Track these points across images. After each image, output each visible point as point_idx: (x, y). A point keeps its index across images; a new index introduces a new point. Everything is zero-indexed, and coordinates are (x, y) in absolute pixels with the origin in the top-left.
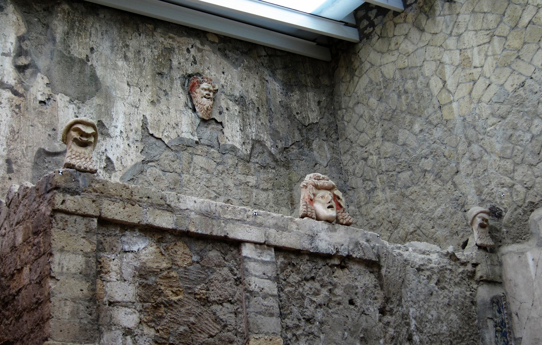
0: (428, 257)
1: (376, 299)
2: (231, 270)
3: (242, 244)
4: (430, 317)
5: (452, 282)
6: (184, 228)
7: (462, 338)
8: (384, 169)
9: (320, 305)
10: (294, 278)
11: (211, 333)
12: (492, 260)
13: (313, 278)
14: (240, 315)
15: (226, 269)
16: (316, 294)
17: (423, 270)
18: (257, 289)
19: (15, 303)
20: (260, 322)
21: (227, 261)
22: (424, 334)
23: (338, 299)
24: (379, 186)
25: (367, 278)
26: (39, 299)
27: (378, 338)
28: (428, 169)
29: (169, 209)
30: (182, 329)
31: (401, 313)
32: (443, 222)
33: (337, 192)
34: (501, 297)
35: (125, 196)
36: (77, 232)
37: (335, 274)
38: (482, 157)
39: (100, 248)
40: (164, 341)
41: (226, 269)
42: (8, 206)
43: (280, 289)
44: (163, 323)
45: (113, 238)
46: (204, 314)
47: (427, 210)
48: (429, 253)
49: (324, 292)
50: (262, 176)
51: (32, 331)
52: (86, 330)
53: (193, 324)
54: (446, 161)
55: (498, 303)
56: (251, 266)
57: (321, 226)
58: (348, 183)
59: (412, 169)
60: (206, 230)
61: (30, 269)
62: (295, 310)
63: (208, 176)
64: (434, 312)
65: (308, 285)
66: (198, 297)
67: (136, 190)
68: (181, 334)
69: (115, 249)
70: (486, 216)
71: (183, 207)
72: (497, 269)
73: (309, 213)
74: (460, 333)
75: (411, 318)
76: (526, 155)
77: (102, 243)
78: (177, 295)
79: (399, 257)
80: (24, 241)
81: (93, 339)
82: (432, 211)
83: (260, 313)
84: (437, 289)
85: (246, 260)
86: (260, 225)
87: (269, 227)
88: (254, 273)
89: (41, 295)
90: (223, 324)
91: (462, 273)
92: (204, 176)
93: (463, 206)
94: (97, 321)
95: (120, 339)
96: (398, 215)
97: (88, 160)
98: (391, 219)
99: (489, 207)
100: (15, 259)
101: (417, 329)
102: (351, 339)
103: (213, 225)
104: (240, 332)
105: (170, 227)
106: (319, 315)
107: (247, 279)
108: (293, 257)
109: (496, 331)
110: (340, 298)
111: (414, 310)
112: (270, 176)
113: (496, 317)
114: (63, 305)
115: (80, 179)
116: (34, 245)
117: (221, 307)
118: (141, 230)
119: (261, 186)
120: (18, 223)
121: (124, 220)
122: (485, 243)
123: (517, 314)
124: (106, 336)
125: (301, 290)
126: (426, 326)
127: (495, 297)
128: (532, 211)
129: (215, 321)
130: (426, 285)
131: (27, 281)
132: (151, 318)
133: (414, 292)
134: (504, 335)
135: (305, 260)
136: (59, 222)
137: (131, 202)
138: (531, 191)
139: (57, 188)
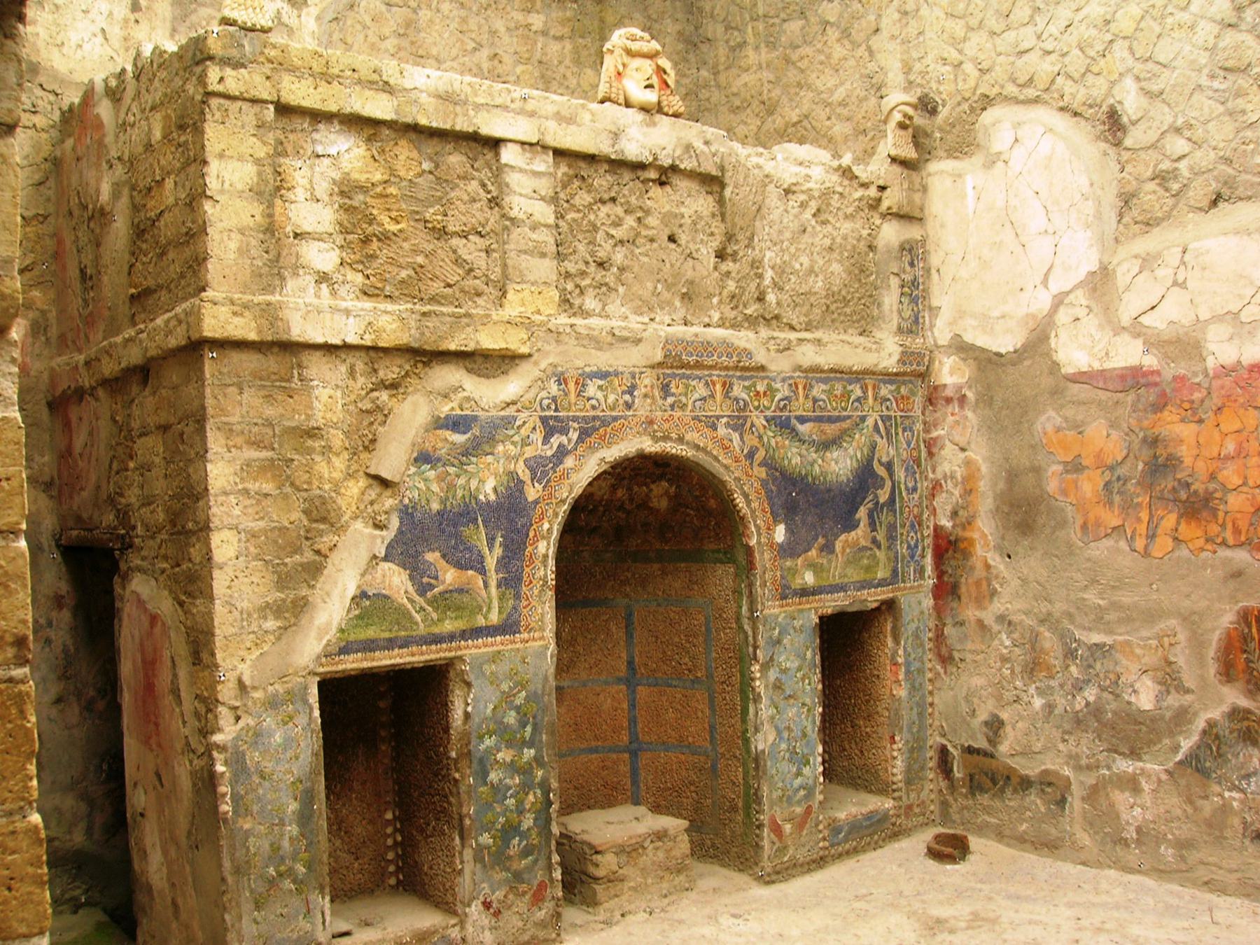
0: (808, 171)
1: (712, 234)
2: (484, 185)
3: (502, 144)
4: (797, 266)
5: (840, 213)
6: (409, 120)
7: (846, 302)
8: (761, 13)
9: (621, 242)
10: (583, 198)
12: (911, 182)
13: (613, 200)
14: (495, 255)
15: (475, 183)
16: (617, 224)
17: (794, 192)
18: (522, 216)
19: (156, 232)
20: (524, 265)
21: (477, 170)
23: (651, 233)
24: (751, 39)
25: (701, 201)
26: (191, 229)
27: (710, 296)
28: (832, 20)
29: (387, 88)
30: (404, 274)
31: (750, 259)
32: (845, 112)
33: (665, 63)
34: (917, 242)
35: (317, 68)
36: (243, 127)
37: (650, 194)
38: (918, 10)
39: (280, 151)
40: (377, 292)
41: (475, 183)
42: (137, 77)
43: (560, 216)
44: (375, 265)
45: (300, 135)
46: (439, 251)
47: (823, 89)
48: (809, 164)
49: (630, 221)
50: (554, 15)
51: (182, 276)
52: (261, 276)
53: (422, 267)
54: (861, 9)
55: (910, 251)
56: (513, 178)
57: (634, 116)
58: (701, 31)
59: (806, 18)
60: (445, 122)
61: (175, 183)
62: (581, 248)
63: (463, 13)
64: (805, 260)
65: (605, 209)
66: (430, 225)
67: (334, 59)
68: (402, 282)
69: (301, 151)
70: (910, 111)
71: (408, 84)
72: (917, 197)
73: (613, 96)
74: (843, 293)
76: (988, 16)
77: (282, 143)
78: (398, 223)
79: (756, 171)
80: (164, 138)
82: (831, 92)
83: (525, 252)
84: (813, 223)
85: (506, 169)
86: (532, 114)
87: (547, 118)
88: (517, 189)
89: (193, 222)
90: (467, 267)
91: (860, 199)
92: (455, 12)
93: (879, 89)
94: (277, 261)
96: (776, 92)
97: (258, 10)
98: (765, 97)
99: (919, 94)
100: (151, 165)
101: (775, 284)
102: (666, 295)
103: (456, 115)
105: (388, 116)
106: (619, 257)
107: (507, 199)
108: (582, 164)
110: (655, 232)
111: (773, 254)
112: (568, 14)
113: (904, 272)
114: (226, 238)
115: (246, 44)
116: (180, 145)
117: (464, 241)
118: (341, 123)
119: (552, 33)
120: (153, 108)
121: (315, 106)
122: (903, 154)
124: (291, 284)
125: (592, 217)
127: (908, 241)
128: (984, 109)
129: (456, 262)
130: (796, 216)
131: (171, 200)
132: (358, 257)
133: (775, 227)
134: (914, 301)
135: (602, 171)
136: (215, 111)
137: (327, 77)
138: (987, 77)
139: (211, 58)
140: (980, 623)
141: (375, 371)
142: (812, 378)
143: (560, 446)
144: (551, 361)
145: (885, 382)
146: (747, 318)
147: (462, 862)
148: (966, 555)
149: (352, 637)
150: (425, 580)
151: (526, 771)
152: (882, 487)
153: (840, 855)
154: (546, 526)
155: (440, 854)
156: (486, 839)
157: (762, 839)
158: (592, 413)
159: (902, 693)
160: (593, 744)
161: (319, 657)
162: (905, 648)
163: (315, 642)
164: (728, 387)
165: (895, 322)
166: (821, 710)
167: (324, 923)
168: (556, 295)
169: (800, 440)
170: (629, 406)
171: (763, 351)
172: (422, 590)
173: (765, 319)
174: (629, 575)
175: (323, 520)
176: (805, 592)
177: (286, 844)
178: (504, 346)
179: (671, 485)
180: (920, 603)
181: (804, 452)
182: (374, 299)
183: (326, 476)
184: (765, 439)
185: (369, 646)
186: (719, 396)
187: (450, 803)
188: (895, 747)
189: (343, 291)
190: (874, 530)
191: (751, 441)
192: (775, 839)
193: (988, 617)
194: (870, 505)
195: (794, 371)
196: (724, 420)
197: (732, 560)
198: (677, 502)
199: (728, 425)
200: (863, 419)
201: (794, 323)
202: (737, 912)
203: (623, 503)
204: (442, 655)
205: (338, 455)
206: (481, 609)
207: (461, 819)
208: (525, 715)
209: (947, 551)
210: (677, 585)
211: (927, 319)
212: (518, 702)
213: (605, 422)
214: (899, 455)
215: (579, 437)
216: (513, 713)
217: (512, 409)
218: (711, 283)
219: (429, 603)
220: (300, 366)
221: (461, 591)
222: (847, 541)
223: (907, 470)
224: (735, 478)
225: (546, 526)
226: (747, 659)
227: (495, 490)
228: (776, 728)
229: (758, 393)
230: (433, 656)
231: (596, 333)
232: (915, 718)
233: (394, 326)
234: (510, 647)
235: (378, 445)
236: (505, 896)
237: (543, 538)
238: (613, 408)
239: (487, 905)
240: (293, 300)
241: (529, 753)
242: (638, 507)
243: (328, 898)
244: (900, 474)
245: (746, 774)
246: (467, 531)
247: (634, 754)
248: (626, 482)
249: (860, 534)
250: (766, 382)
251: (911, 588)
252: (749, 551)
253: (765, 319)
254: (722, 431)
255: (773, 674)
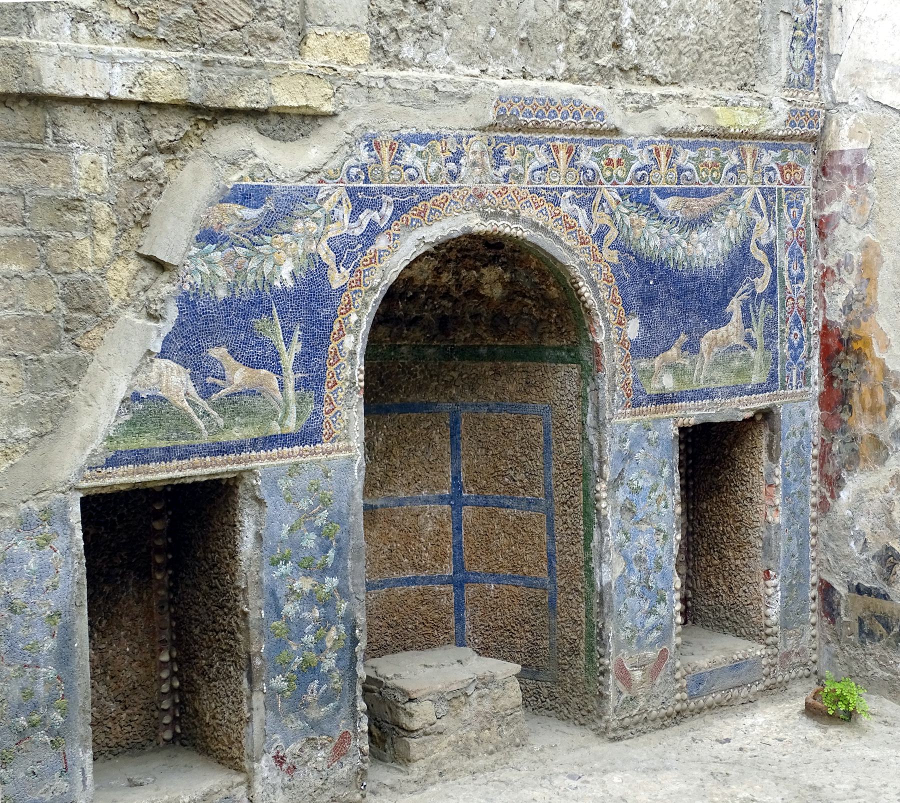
11: (236, 22)
22: (647, 37)
27: (557, 41)
30: (181, 13)
40: (148, 34)
75: (626, 6)
81: (17, 28)
95: (66, 29)
101: (636, 27)
102: (501, 41)
104: (290, 22)
109: (794, 38)
123: (841, 9)
126: (654, 21)
134: (809, 46)
140: (874, 437)
141: (148, 131)
142: (677, 143)
143: (372, 223)
144: (359, 122)
145: (767, 149)
146: (600, 69)
147: (251, 709)
148: (860, 357)
149: (122, 447)
150: (210, 380)
151: (327, 604)
152: (759, 274)
153: (701, 710)
154: (354, 318)
155: (225, 701)
156: (279, 682)
157: (608, 687)
158: (410, 185)
159: (778, 518)
160: (411, 574)
161: (82, 470)
162: (784, 470)
163: (77, 453)
164: (573, 154)
165: (784, 73)
166: (679, 537)
167: (84, 782)
168: (366, 40)
169: (660, 218)
170: (454, 176)
171: (618, 111)
172: (206, 392)
173: (622, 70)
174: (455, 375)
175: (87, 308)
176: (662, 399)
177: (40, 688)
178: (303, 102)
179: (505, 270)
180: (803, 413)
181: (665, 232)
182: (144, 43)
183: (90, 257)
184: (618, 217)
185: (141, 457)
186: (562, 165)
187: (237, 641)
188: (769, 583)
189: (106, 33)
190: (748, 326)
191: (601, 218)
192: (622, 688)
193: (884, 436)
194: (744, 296)
195: (656, 134)
196: (569, 194)
197: (577, 360)
198: (513, 291)
199: (573, 200)
200: (739, 192)
201: (657, 75)
202: (576, 770)
203: (449, 290)
204: (229, 467)
205: (103, 231)
206: (275, 413)
207: (249, 659)
208: (327, 538)
209: (838, 352)
210: (510, 388)
211: (824, 69)
212: (318, 523)
213: (425, 196)
214: (782, 235)
215: (393, 214)
216: (313, 536)
217: (315, 178)
218: (555, 28)
219: (215, 407)
220: (54, 124)
221: (252, 393)
222: (716, 338)
223: (791, 254)
224: (581, 263)
225: (354, 318)
226: (593, 476)
227: (293, 275)
228: (626, 558)
229: (611, 160)
230: (218, 469)
231: (415, 88)
232: (794, 549)
233: (170, 77)
234: (309, 458)
235: (152, 220)
236: (301, 750)
237: (350, 331)
238: (434, 179)
239: (280, 760)
240: (45, 43)
241: (332, 582)
242: (467, 295)
243: (90, 752)
244: (783, 258)
245: (589, 611)
246: (259, 323)
247: (460, 586)
248: (452, 265)
249: (732, 331)
250: (620, 148)
251: (792, 395)
252: (596, 349)
253: (622, 70)
254: (566, 207)
255: (621, 495)
